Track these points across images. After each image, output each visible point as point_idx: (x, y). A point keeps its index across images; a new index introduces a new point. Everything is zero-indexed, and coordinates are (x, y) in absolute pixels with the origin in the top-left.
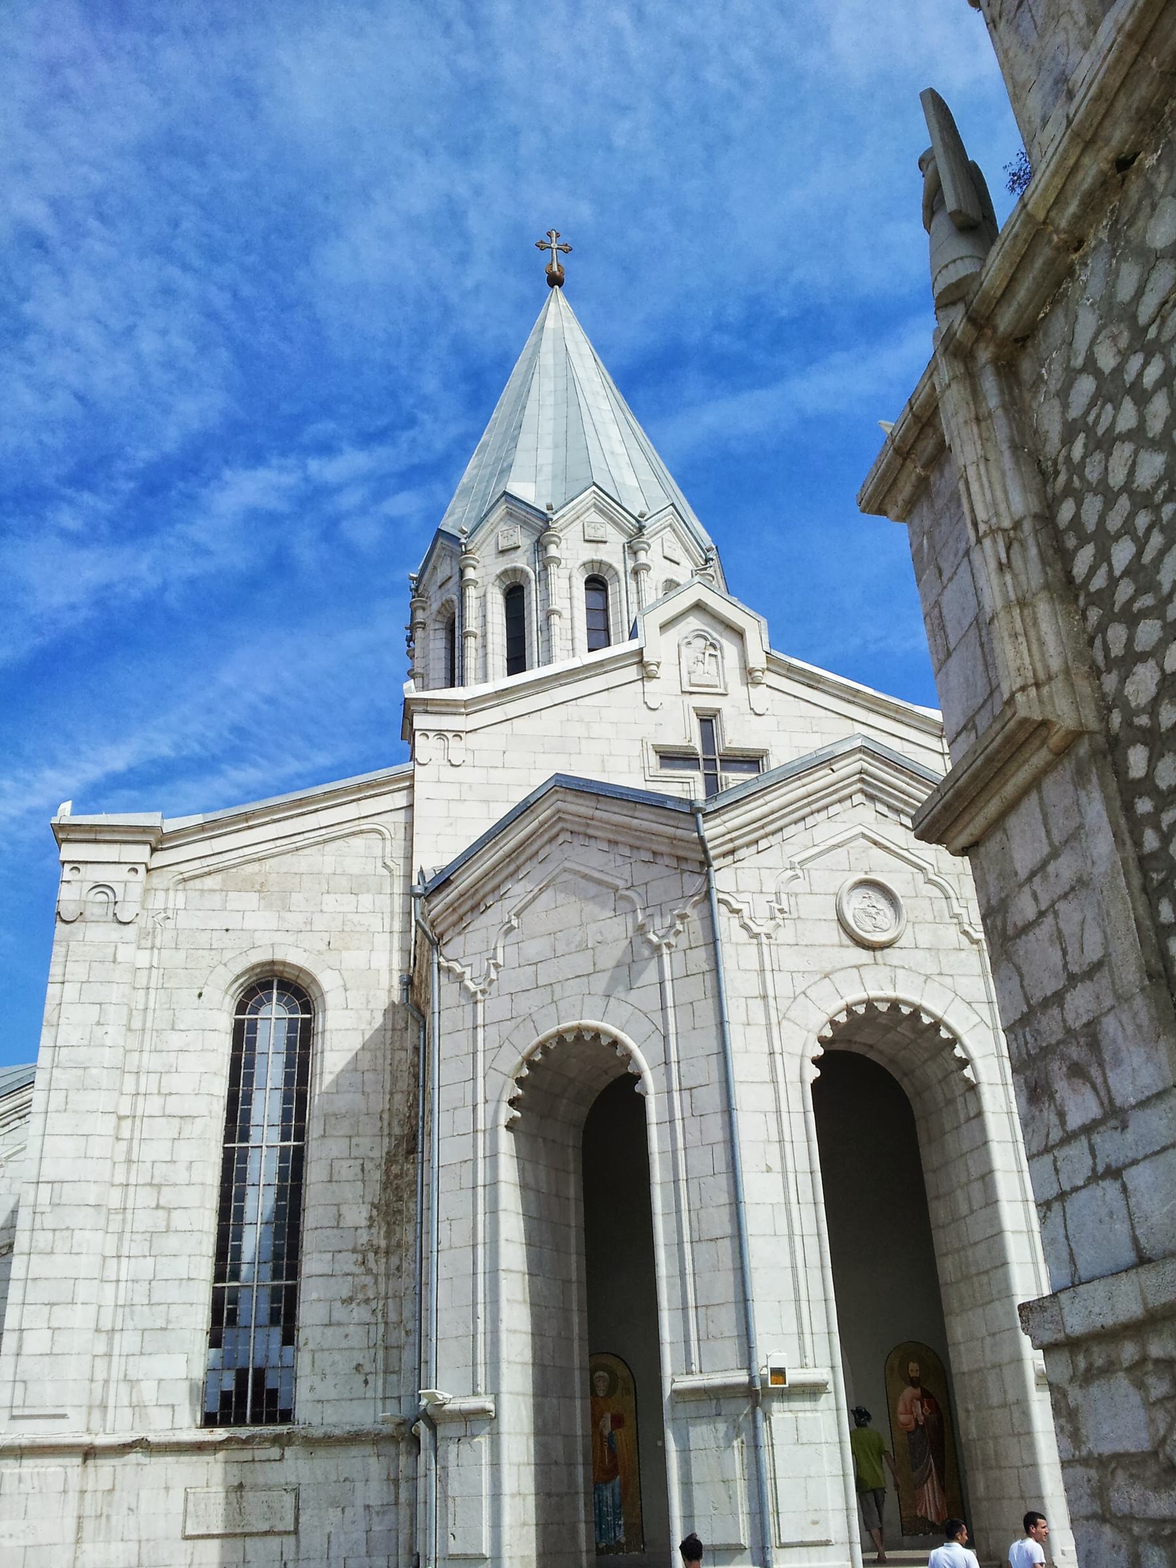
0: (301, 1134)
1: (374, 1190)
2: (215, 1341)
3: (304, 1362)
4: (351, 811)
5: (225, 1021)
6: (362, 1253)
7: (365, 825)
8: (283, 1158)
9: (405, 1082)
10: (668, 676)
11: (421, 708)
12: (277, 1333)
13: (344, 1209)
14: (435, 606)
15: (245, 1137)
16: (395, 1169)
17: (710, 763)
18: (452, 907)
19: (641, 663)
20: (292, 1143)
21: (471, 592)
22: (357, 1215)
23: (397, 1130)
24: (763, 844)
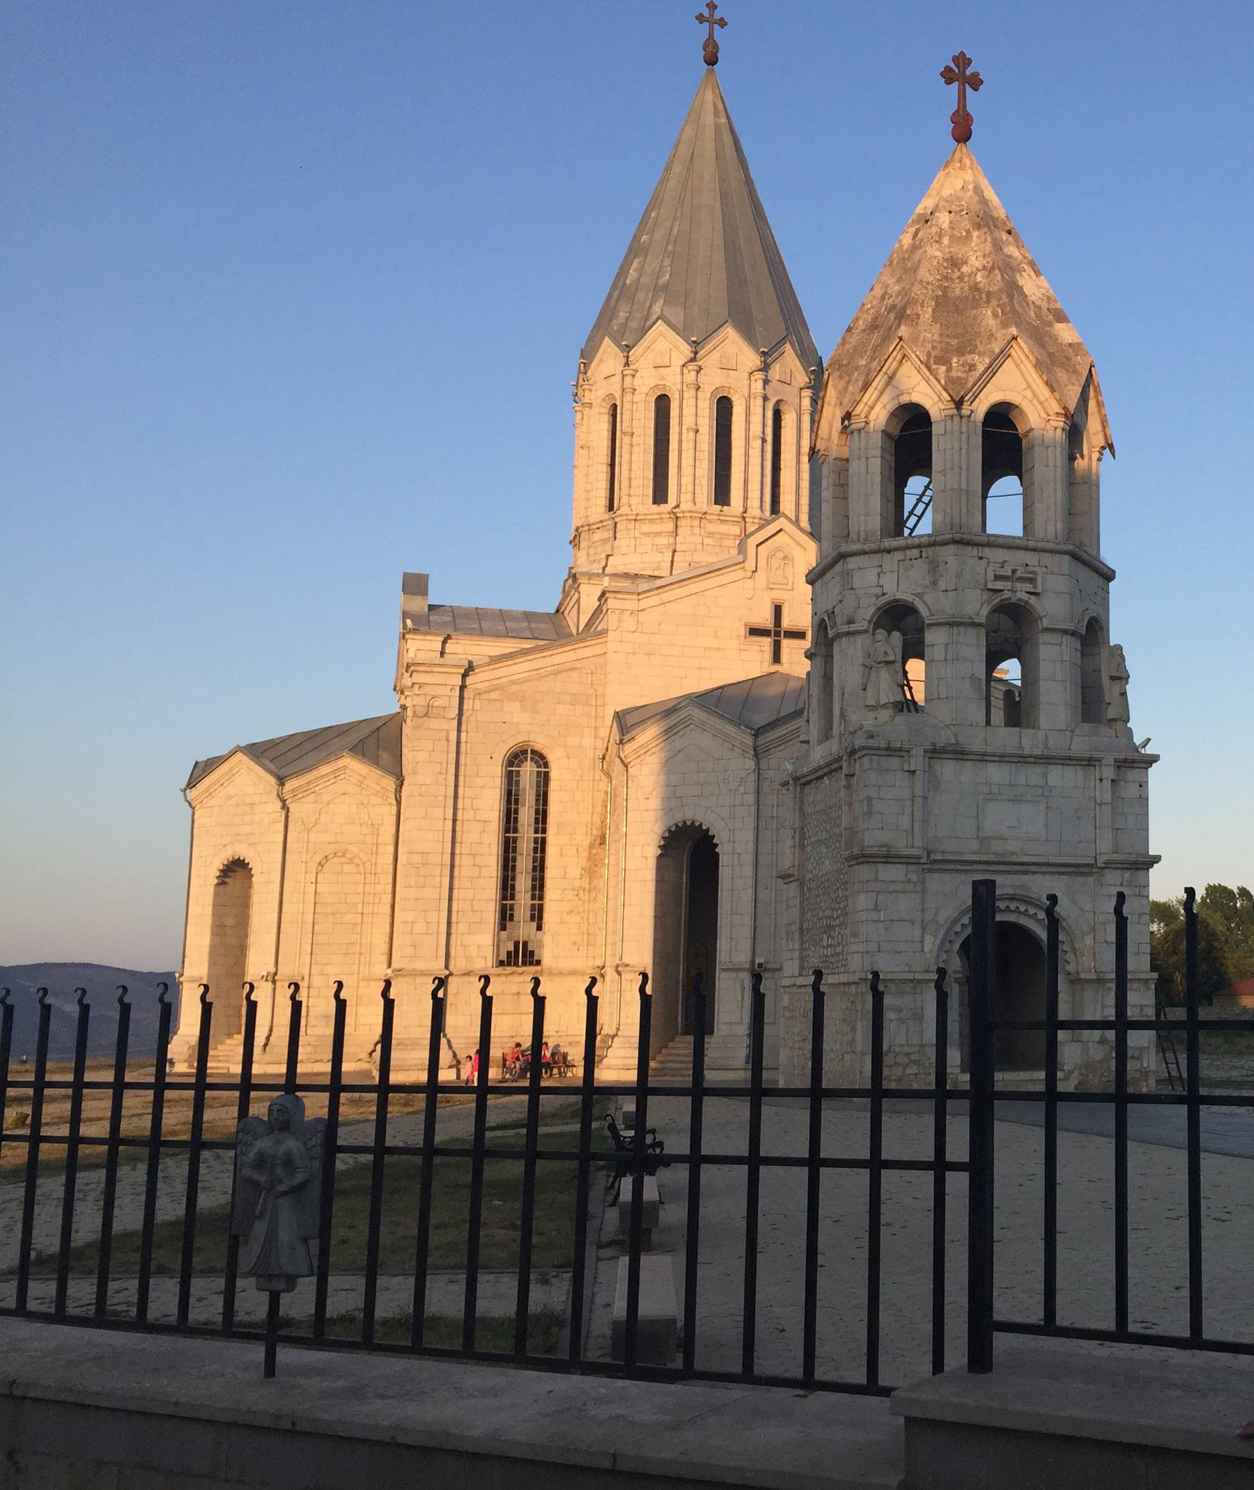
0: (544, 831)
1: (583, 862)
4: (571, 656)
6: (578, 891)
7: (579, 664)
9: (599, 809)
11: (613, 595)
12: (534, 924)
14: (601, 393)
16: (594, 851)
17: (777, 634)
20: (539, 835)
21: (628, 397)
22: (575, 872)
23: (595, 832)
24: (782, 747)
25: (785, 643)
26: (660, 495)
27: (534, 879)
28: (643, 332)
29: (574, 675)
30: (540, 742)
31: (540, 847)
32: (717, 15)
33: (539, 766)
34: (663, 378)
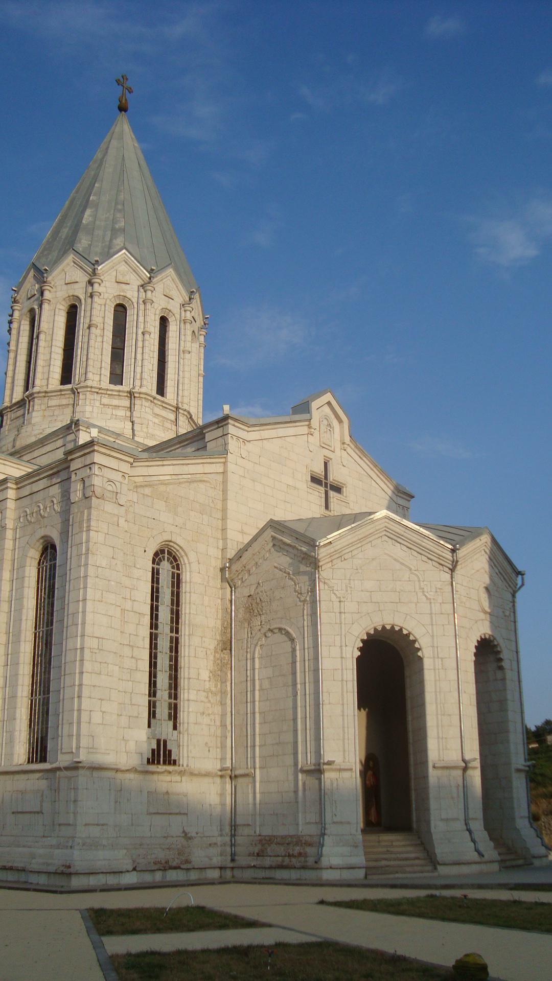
0: (177, 632)
2: (149, 726)
3: (184, 739)
4: (199, 469)
5: (150, 565)
7: (205, 478)
8: (171, 642)
10: (316, 433)
12: (171, 723)
13: (201, 671)
15: (156, 628)
17: (326, 486)
18: (330, 555)
19: (309, 426)
22: (205, 675)
25: (332, 494)
26: (117, 377)
27: (170, 678)
28: (108, 254)
29: (202, 485)
30: (179, 541)
31: (175, 646)
32: (128, 84)
33: (173, 568)
34: (123, 291)
